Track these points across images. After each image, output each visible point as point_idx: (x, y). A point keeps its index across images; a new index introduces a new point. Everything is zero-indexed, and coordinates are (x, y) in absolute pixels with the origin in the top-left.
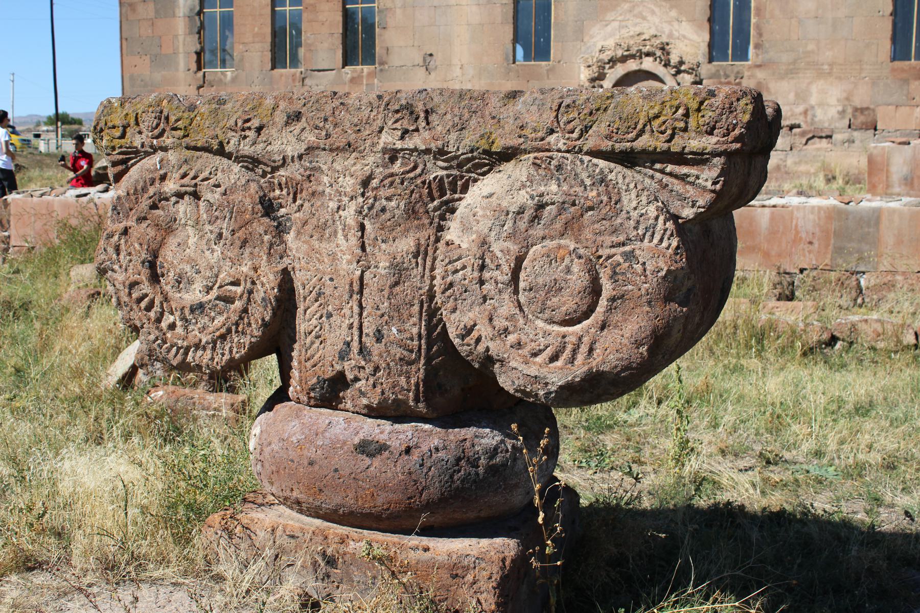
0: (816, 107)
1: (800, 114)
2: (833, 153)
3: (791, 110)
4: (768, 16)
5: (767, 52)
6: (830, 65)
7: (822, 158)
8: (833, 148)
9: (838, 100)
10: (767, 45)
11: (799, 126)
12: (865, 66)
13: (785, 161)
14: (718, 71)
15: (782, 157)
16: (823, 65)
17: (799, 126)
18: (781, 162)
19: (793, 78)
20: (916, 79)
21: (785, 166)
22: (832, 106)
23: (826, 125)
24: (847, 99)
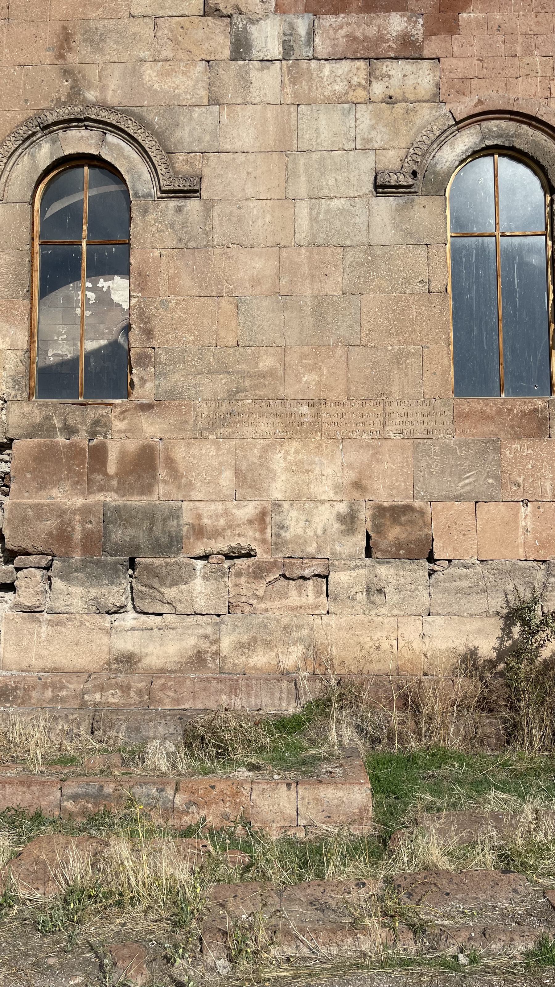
0: (286, 506)
1: (250, 522)
2: (332, 620)
3: (226, 512)
4: (164, 290)
5: (161, 374)
6: (312, 405)
7: (306, 632)
8: (332, 609)
9: (337, 488)
10: (164, 358)
11: (249, 554)
12: (394, 407)
13: (216, 641)
14: (48, 418)
15: (209, 630)
16: (298, 403)
17: (249, 554)
18: (205, 645)
19: (229, 437)
20: (515, 437)
21: (217, 653)
22: (323, 502)
23: (311, 549)
24: (357, 485)
